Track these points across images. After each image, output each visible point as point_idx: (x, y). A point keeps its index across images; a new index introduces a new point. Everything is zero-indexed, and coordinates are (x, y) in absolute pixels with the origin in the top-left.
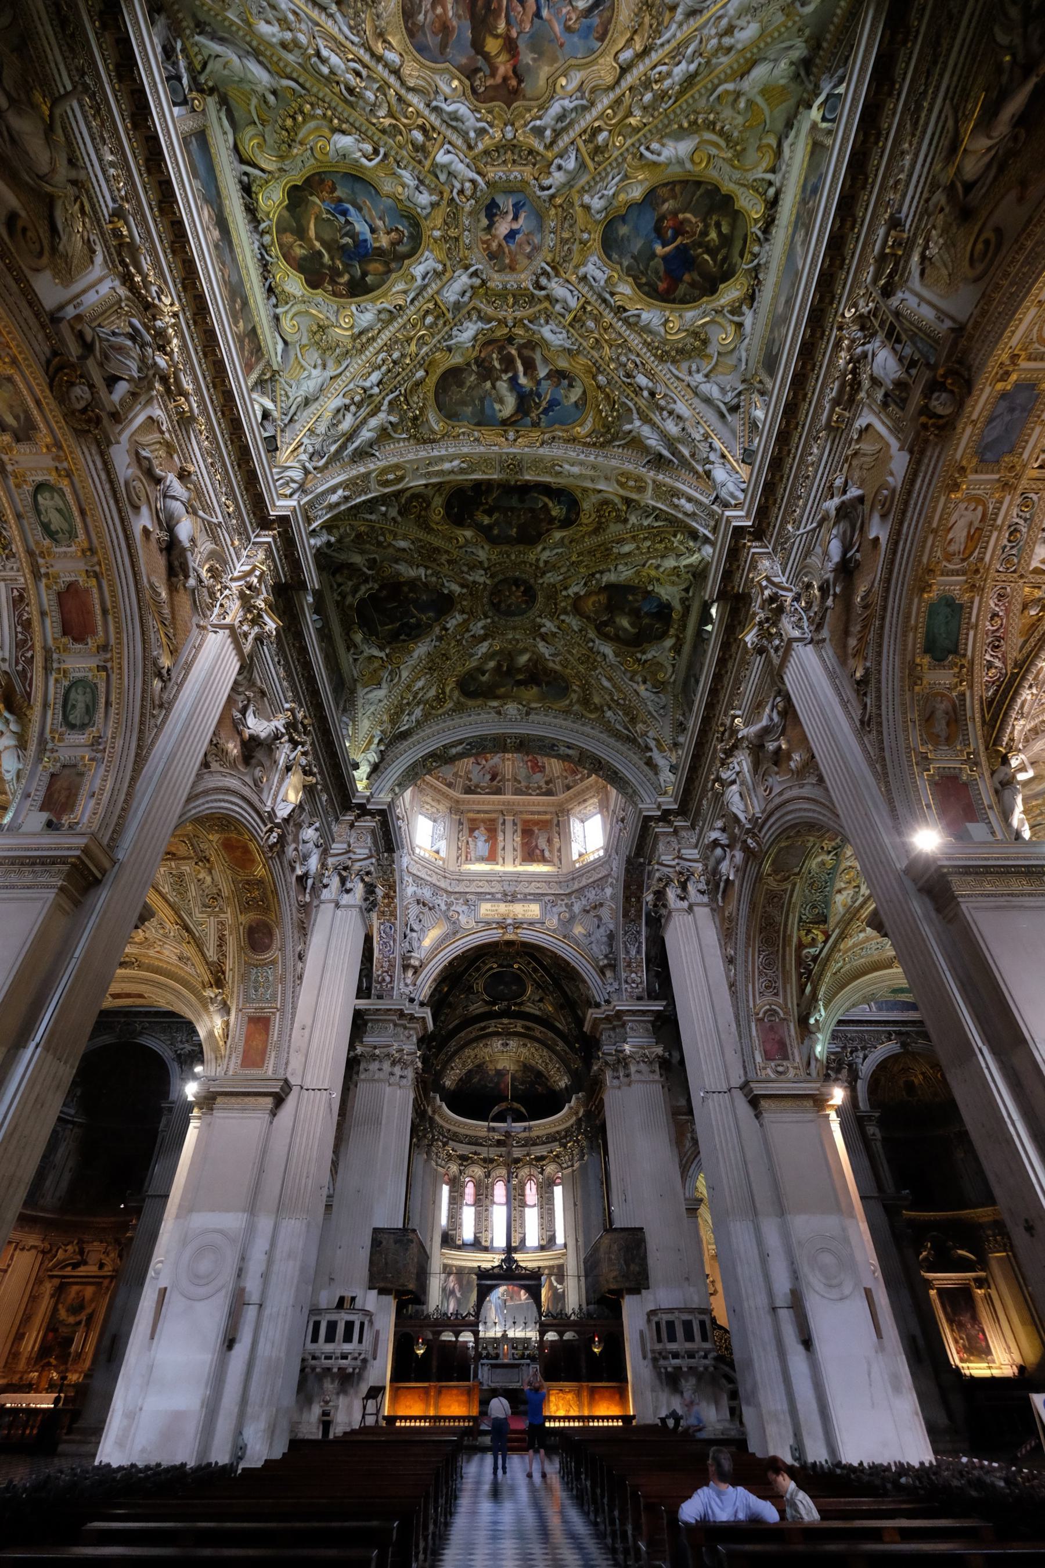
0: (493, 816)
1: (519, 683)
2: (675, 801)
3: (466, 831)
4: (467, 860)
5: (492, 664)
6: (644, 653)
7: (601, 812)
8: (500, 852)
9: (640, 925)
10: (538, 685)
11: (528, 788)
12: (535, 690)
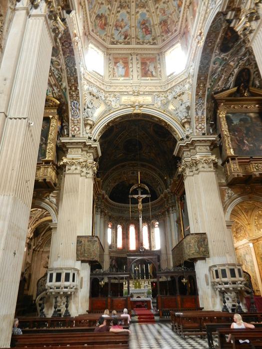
0: (127, 56)
3: (113, 63)
9: (204, 99)
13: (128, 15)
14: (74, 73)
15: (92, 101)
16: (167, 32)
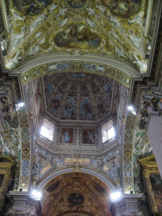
0: (72, 128)
1: (80, 40)
3: (61, 132)
6: (131, 20)
7: (114, 126)
8: (74, 140)
12: (86, 43)
13: (75, 101)
14: (28, 141)
15: (41, 161)
16: (103, 112)
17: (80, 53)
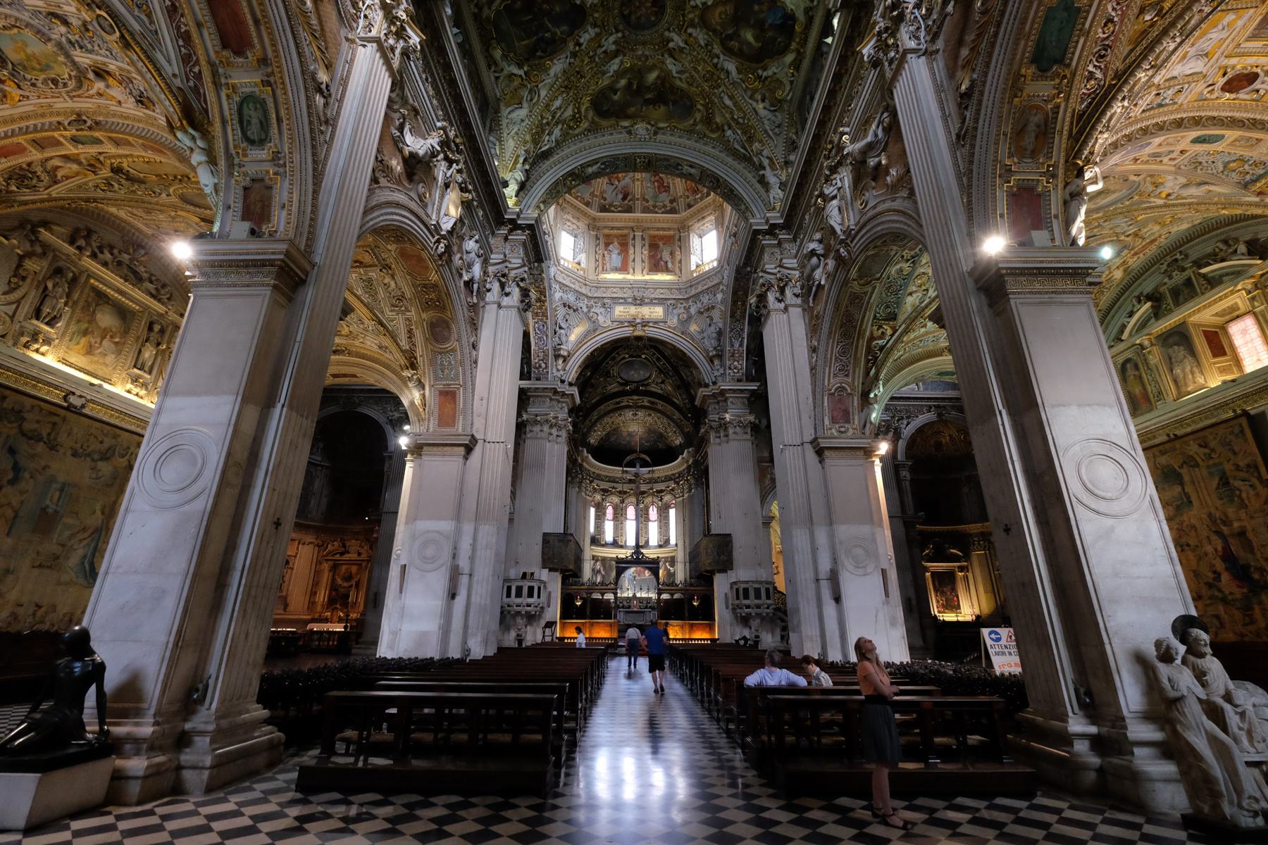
0: (625, 232)
1: (648, 102)
2: (782, 216)
3: (602, 245)
4: (604, 270)
5: (623, 82)
6: (765, 69)
7: (717, 228)
8: (631, 264)
9: (744, 324)
10: (666, 104)
11: (655, 206)
12: (663, 108)
17: (647, 129)
